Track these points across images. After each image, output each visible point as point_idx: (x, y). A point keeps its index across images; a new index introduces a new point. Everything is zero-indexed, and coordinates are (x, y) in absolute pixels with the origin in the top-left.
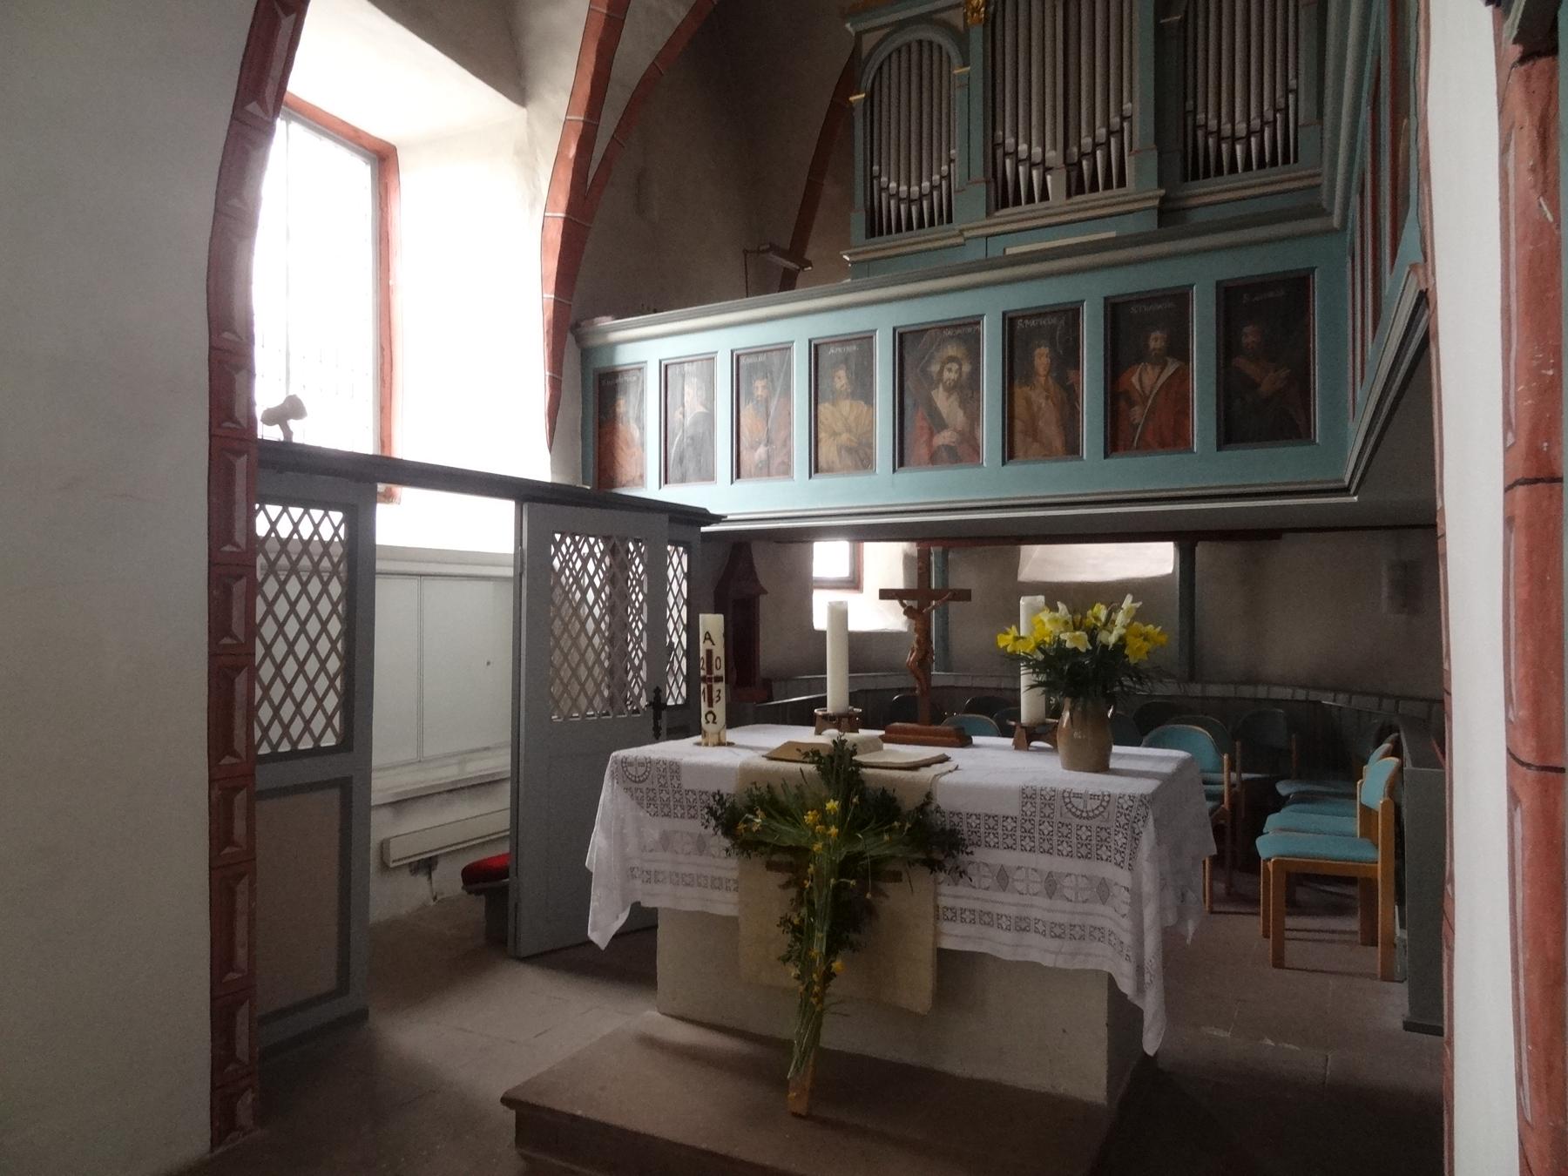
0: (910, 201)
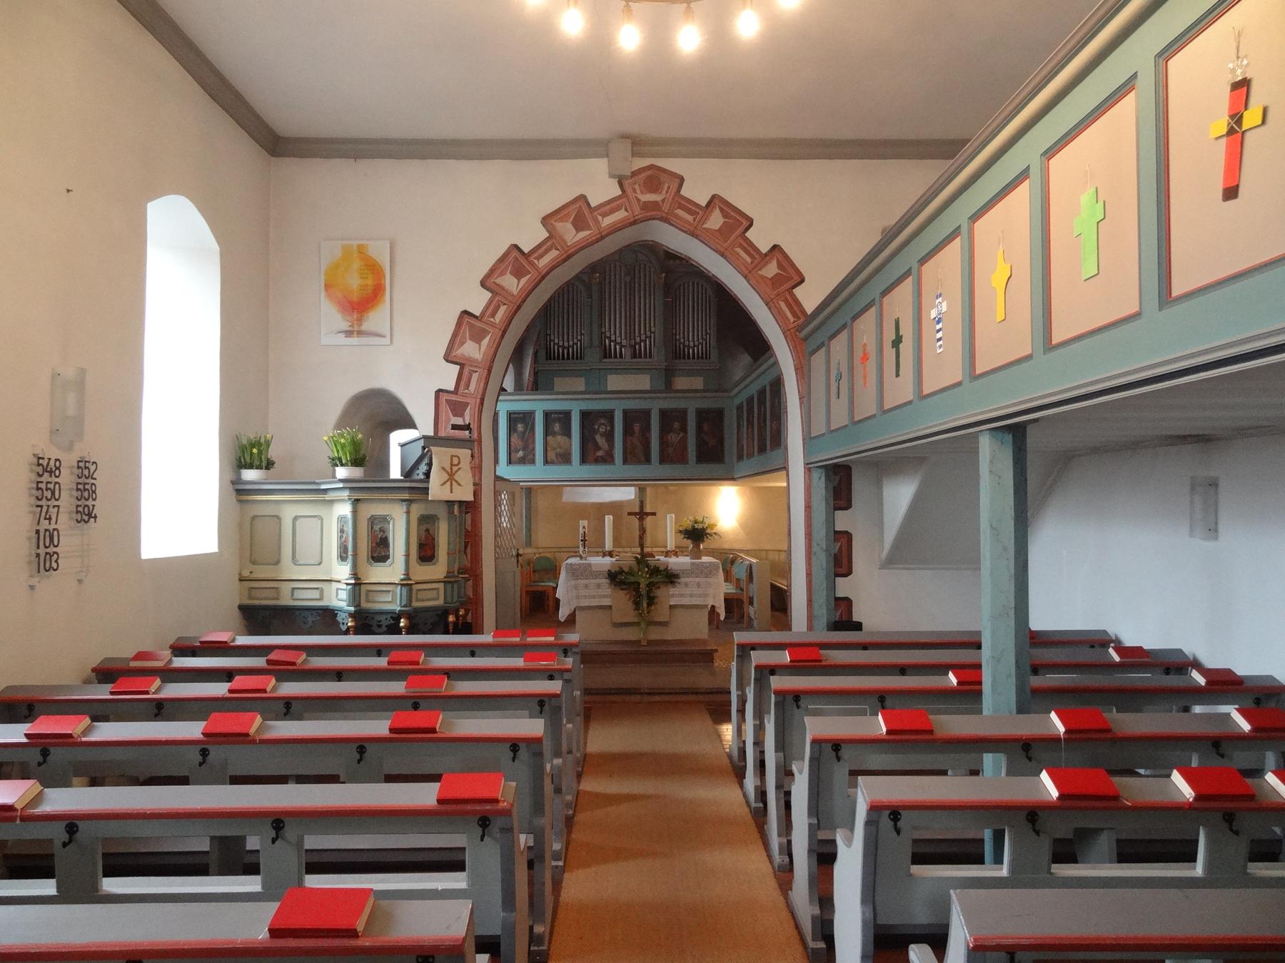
0: (563, 347)
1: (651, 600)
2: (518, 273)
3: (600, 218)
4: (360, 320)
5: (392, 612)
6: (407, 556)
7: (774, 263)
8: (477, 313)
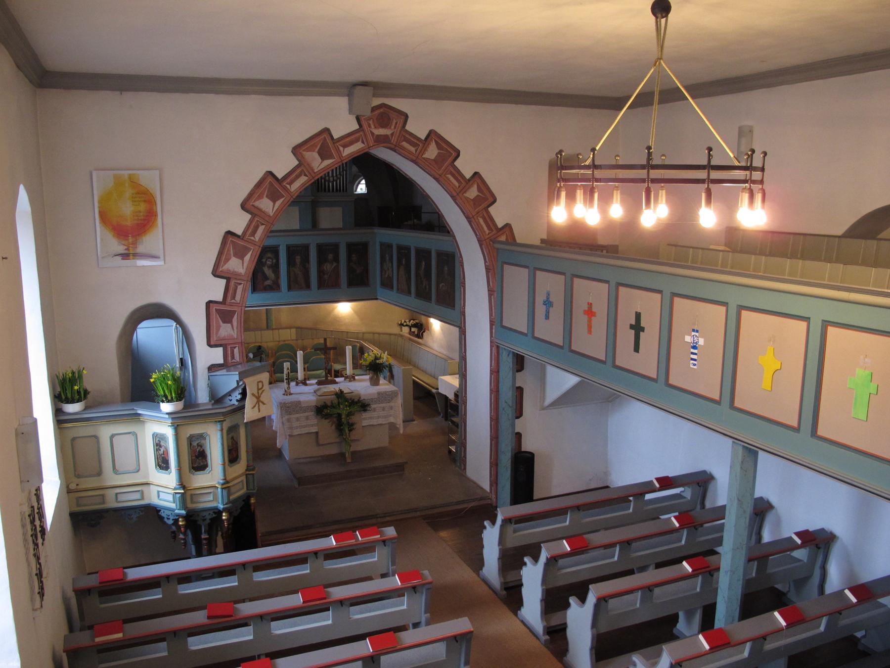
1: (351, 427)
2: (274, 197)
3: (341, 149)
4: (135, 244)
7: (475, 186)
8: (239, 233)
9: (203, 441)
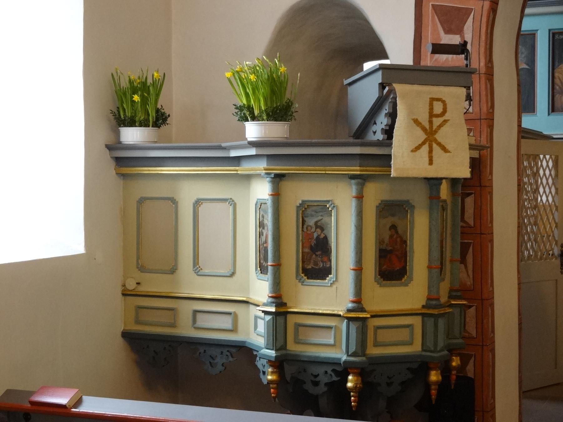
5: (334, 363)
6: (359, 270)
9: (326, 219)
